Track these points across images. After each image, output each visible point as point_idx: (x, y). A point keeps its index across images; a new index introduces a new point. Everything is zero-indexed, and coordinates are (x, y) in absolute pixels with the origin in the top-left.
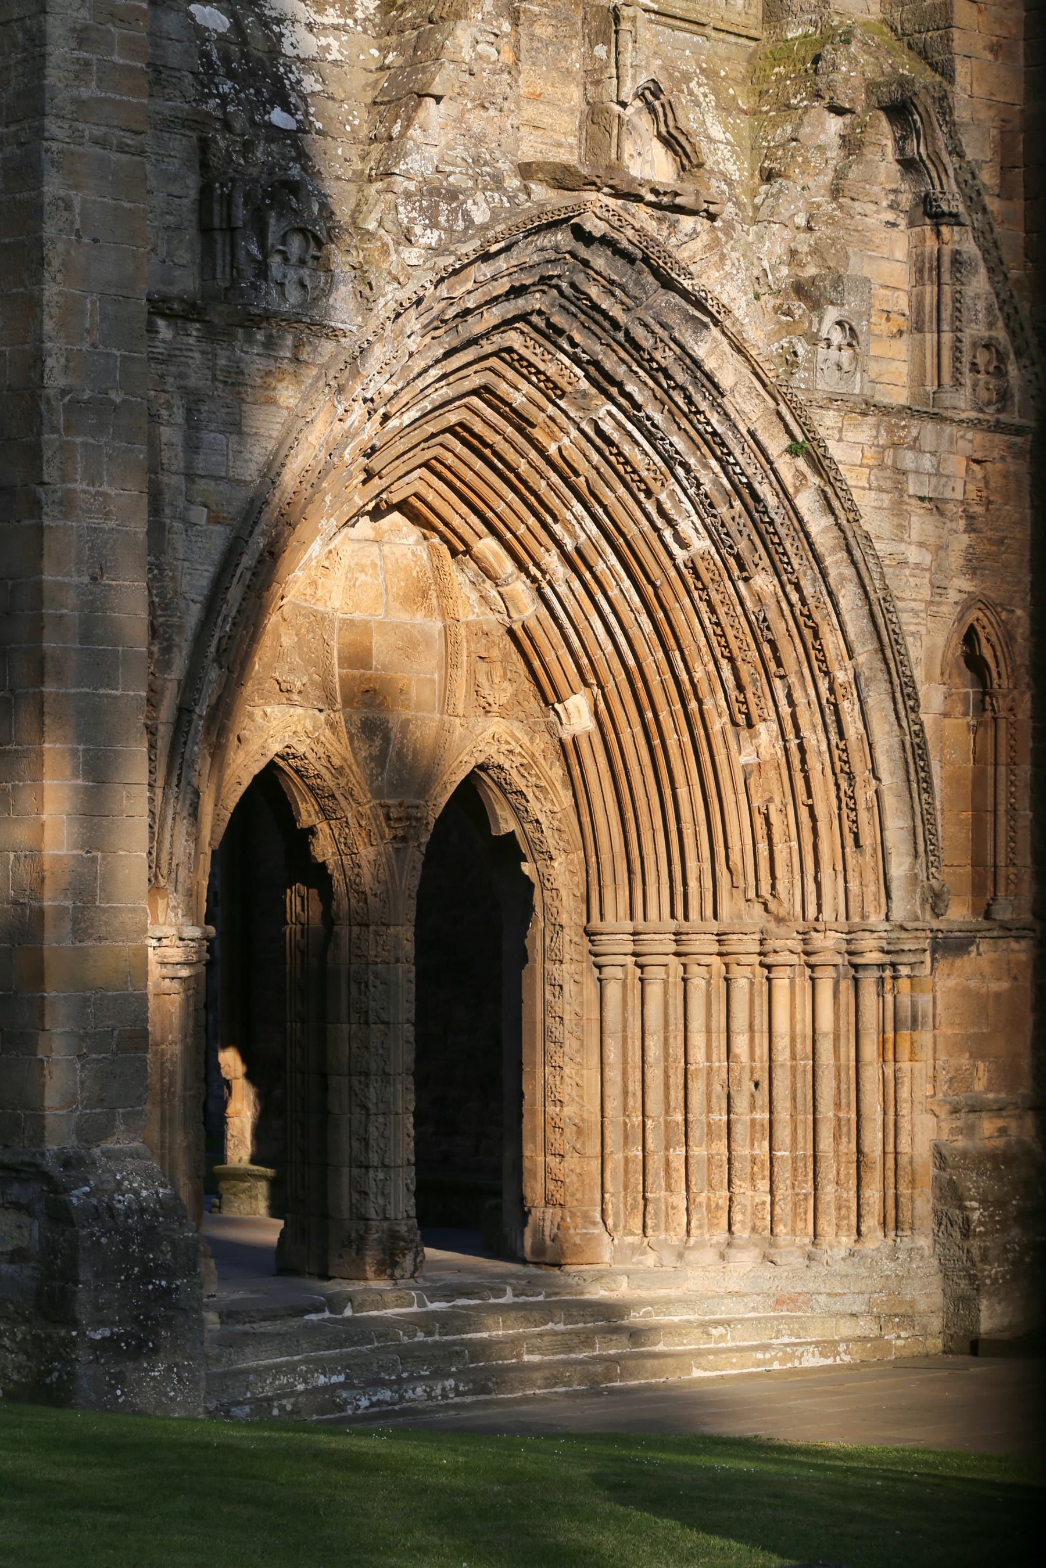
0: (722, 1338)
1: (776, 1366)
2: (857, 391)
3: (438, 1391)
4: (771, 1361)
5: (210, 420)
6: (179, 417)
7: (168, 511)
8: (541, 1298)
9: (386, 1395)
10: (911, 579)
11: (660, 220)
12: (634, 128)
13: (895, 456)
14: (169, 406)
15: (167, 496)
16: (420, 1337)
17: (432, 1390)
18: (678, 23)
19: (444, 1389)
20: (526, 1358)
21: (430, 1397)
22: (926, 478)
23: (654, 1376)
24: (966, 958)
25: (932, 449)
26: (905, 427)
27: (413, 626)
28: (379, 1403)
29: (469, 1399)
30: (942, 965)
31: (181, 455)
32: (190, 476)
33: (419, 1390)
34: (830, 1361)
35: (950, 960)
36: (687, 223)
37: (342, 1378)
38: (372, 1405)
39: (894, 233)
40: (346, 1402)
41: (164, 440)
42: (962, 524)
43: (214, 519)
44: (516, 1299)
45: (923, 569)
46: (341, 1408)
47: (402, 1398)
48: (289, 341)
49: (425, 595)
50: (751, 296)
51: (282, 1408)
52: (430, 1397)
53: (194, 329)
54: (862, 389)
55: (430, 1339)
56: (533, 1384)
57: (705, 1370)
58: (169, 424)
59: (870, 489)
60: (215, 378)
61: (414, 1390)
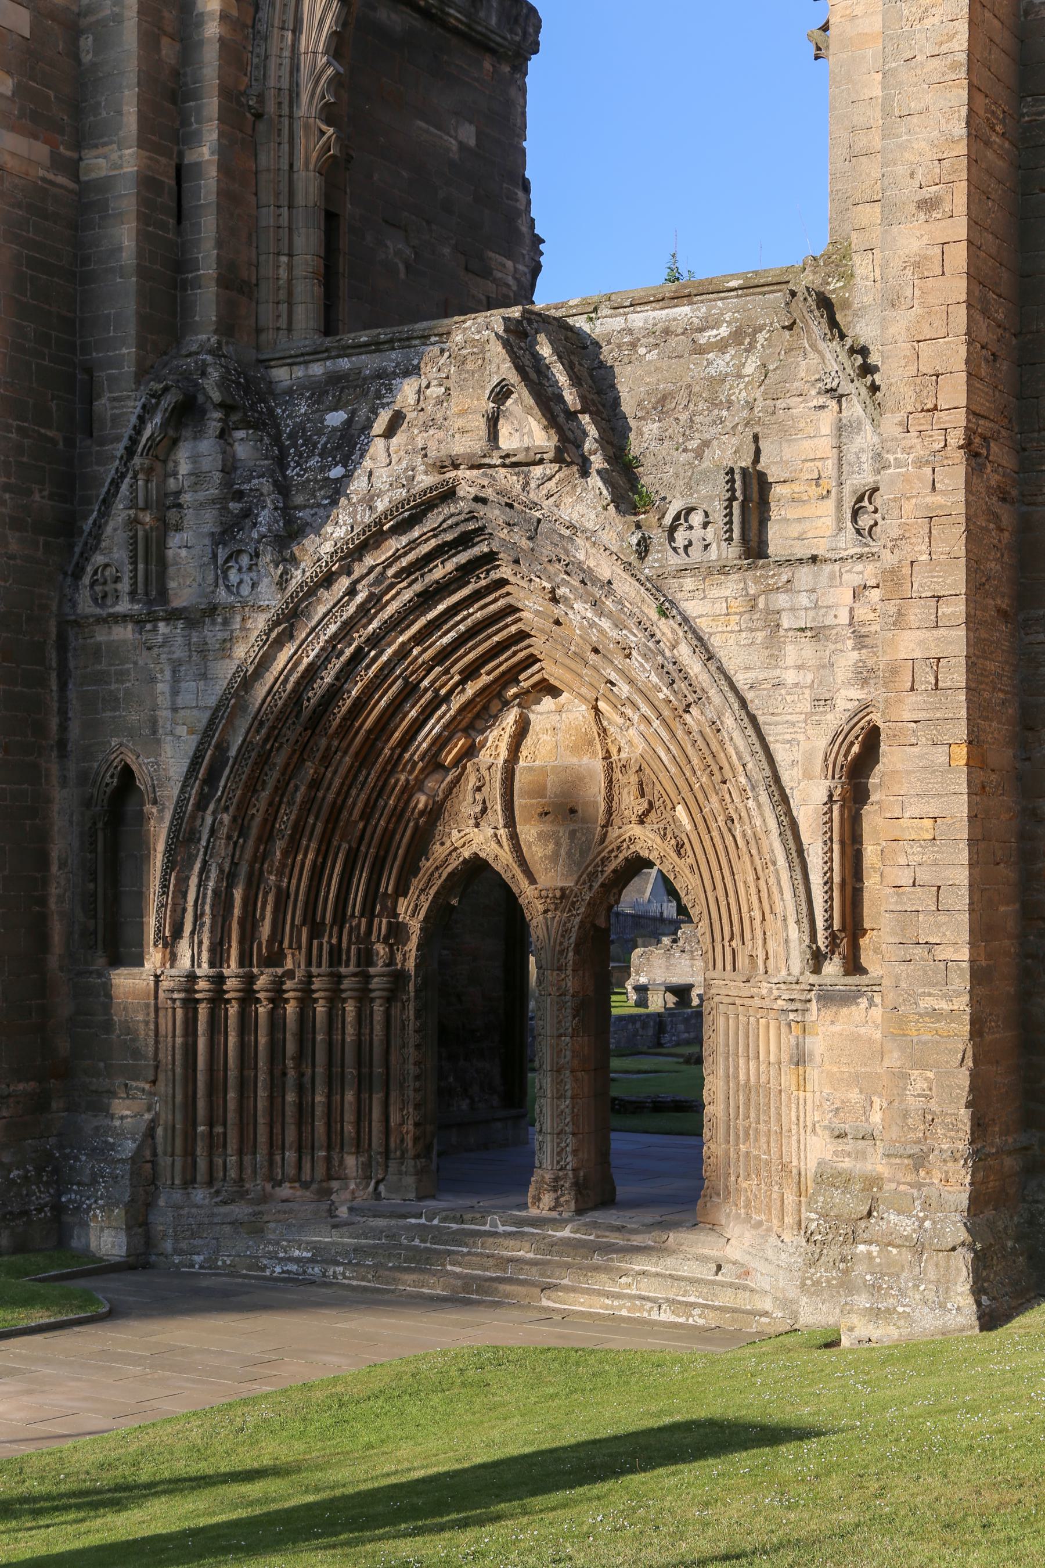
0: (629, 1285)
1: (624, 1313)
2: (714, 557)
3: (331, 1273)
4: (620, 1308)
5: (186, 675)
6: (168, 675)
7: (161, 731)
8: (592, 1238)
9: (294, 1267)
10: (788, 697)
11: (517, 474)
12: (511, 413)
13: (767, 600)
14: (162, 671)
15: (161, 723)
16: (417, 1242)
17: (326, 1271)
18: (766, 289)
19: (334, 1272)
20: (449, 1268)
21: (324, 1275)
22: (803, 613)
23: (507, 1297)
24: (854, 1008)
25: (809, 588)
26: (774, 575)
27: (580, 766)
28: (288, 1272)
29: (355, 1283)
30: (828, 1014)
31: (168, 698)
32: (175, 709)
33: (316, 1269)
34: (682, 1320)
35: (834, 1009)
36: (537, 471)
37: (309, 1255)
38: (283, 1272)
40: (266, 1266)
41: (158, 691)
42: (850, 643)
43: (191, 732)
44: (573, 1235)
45: (802, 687)
46: (263, 1269)
47: (305, 1272)
48: (238, 618)
49: (591, 743)
50: (600, 509)
51: (224, 1262)
52: (324, 1275)
53: (180, 624)
54: (719, 555)
55: (423, 1245)
56: (404, 1283)
57: (555, 1302)
58: (162, 681)
59: (740, 631)
60: (190, 650)
61: (313, 1269)
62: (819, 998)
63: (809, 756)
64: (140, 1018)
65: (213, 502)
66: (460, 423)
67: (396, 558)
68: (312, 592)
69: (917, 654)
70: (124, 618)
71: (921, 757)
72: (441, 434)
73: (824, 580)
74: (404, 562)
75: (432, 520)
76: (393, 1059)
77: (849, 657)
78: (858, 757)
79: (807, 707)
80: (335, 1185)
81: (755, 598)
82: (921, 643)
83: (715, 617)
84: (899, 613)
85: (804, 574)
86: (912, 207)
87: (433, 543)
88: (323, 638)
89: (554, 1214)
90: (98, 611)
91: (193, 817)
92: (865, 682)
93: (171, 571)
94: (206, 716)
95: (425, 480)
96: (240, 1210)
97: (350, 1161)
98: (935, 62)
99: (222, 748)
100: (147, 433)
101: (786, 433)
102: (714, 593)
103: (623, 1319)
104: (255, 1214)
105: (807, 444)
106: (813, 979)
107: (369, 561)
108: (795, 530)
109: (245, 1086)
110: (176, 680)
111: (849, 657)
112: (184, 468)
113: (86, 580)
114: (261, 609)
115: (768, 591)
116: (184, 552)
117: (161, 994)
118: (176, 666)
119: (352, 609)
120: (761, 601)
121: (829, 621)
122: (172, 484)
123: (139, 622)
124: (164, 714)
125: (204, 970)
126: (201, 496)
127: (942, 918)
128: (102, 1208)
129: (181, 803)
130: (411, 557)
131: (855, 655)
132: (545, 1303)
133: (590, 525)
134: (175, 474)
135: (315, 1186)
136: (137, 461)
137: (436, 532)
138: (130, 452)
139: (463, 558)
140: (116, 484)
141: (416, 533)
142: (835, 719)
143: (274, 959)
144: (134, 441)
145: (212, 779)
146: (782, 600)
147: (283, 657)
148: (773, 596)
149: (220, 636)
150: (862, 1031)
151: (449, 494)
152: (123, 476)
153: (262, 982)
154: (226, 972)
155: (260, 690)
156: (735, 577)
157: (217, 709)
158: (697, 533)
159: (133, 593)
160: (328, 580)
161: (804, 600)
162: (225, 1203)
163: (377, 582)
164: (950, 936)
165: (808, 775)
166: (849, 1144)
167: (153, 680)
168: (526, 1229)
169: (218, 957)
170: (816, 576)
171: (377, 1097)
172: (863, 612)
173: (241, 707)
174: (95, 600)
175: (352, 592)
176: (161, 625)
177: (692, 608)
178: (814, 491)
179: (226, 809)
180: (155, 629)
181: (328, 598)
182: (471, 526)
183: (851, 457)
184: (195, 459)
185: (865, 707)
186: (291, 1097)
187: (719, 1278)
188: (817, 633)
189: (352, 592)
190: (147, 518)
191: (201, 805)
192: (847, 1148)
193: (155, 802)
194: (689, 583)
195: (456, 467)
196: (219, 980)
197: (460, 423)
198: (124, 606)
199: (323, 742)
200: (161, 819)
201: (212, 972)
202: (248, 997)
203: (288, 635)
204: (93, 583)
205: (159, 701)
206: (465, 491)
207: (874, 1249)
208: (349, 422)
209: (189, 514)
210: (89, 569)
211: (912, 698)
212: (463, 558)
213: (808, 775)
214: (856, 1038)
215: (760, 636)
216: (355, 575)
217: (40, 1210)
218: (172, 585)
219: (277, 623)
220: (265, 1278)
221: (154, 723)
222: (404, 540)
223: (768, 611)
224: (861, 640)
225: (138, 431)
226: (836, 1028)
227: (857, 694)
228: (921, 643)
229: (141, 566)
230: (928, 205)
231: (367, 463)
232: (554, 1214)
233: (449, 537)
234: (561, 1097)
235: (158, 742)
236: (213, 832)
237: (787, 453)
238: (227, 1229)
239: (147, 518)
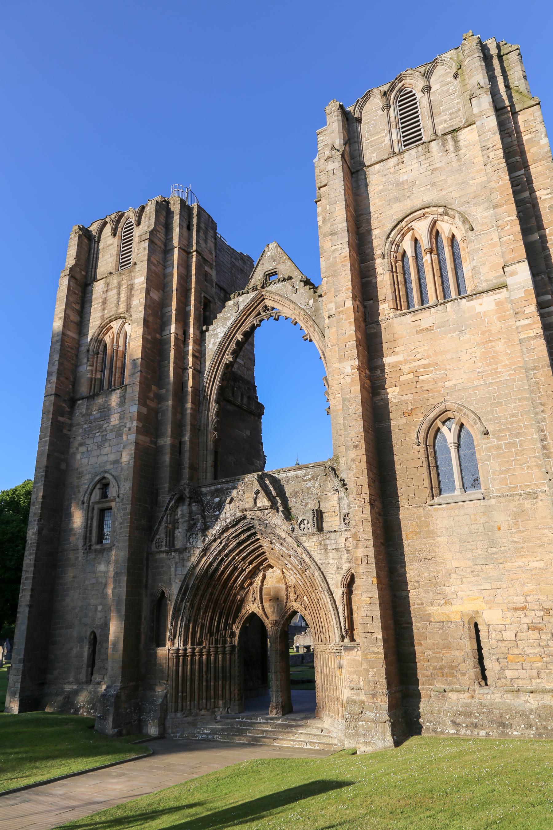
0: (298, 737)
1: (297, 746)
4: (295, 744)
6: (174, 566)
9: (205, 736)
16: (239, 726)
30: (347, 653)
32: (176, 575)
34: (313, 748)
36: (266, 511)
39: (335, 495)
42: (345, 552)
43: (180, 581)
46: (196, 737)
49: (282, 580)
53: (178, 553)
62: (344, 649)
63: (337, 583)
64: (164, 662)
65: (187, 521)
66: (247, 500)
67: (232, 534)
68: (211, 543)
69: (362, 555)
70: (163, 552)
71: (365, 581)
72: (242, 503)
73: (338, 537)
74: (234, 535)
75: (241, 524)
76: (232, 671)
77: (346, 556)
78: (349, 582)
79: (335, 569)
80: (216, 710)
81: (321, 541)
82: (363, 552)
83: (311, 546)
84: (357, 544)
85: (333, 535)
86: (352, 447)
87: (241, 530)
88: (214, 555)
89: (276, 716)
90: (157, 550)
91: (180, 604)
92: (350, 562)
93: (176, 539)
94: (184, 576)
95: (239, 514)
96: (190, 719)
97: (221, 702)
98: (355, 415)
99: (187, 585)
100: (171, 505)
101: (326, 500)
102: (311, 540)
103: (296, 748)
104: (194, 720)
105: (331, 503)
106: (342, 643)
107: (225, 535)
108: (330, 524)
109: (192, 681)
110: (176, 567)
111: (346, 556)
112: (180, 513)
113: (154, 542)
114: (198, 548)
115: (324, 540)
116: (179, 534)
117: (170, 655)
118: (176, 563)
119: (221, 547)
120: (323, 542)
121: (340, 547)
122: (176, 517)
123: (167, 552)
124: (173, 576)
125: (182, 647)
126: (184, 520)
127: (374, 625)
128: (152, 720)
129: (177, 600)
130: (236, 534)
131: (347, 555)
132: (275, 744)
133: (279, 524)
134: (177, 515)
135: (211, 710)
136: (168, 512)
137: (242, 527)
138: (166, 509)
139: (248, 533)
140: (162, 518)
141: (237, 528)
142: (343, 572)
143: (200, 643)
144: (167, 507)
145: (184, 594)
146: (328, 542)
147: (203, 560)
148: (325, 541)
149: (188, 555)
150: (356, 658)
151: (245, 518)
152: (164, 515)
153: (197, 650)
154: (187, 647)
155: (198, 569)
156: (316, 536)
157: (187, 574)
158: (306, 525)
159: (166, 546)
160: (215, 540)
161: (333, 541)
162: (186, 717)
163: (227, 540)
164: (377, 630)
165: (337, 587)
166: (355, 692)
167: (170, 568)
168: (269, 721)
169: (185, 644)
170: (336, 535)
171: (228, 683)
172: (348, 544)
173: (193, 574)
174: (156, 547)
175: (221, 543)
176: (173, 553)
177: (305, 544)
178: (334, 514)
179: (188, 602)
180: (171, 554)
181: (215, 545)
182: (250, 525)
183: (342, 506)
184: (182, 511)
185: (350, 569)
186: (204, 684)
187: (322, 734)
188: (337, 550)
189: (221, 543)
190: (170, 526)
191: (182, 601)
192: (355, 692)
193: (170, 600)
194: (305, 538)
195: (246, 511)
196: (185, 650)
197: (247, 500)
198: (164, 549)
199: (213, 583)
200: (171, 605)
201: (184, 648)
202: (193, 655)
203: (205, 555)
204: (156, 543)
205: (172, 573)
206: (249, 517)
207: (364, 723)
208: (220, 501)
209: (180, 524)
210: (155, 539)
211: (362, 566)
212: (248, 533)
213: (337, 587)
214: (354, 660)
215: (323, 551)
216: (222, 539)
217: (134, 721)
218: (176, 543)
219: (202, 552)
220: (197, 740)
221: (170, 579)
222: (234, 529)
223: (324, 545)
224: (348, 551)
225: (169, 504)
226: (349, 657)
227: (348, 565)
228: (363, 552)
229: (168, 538)
230: (356, 447)
231: (225, 511)
232: (276, 716)
233: (245, 528)
234: (277, 680)
235: (171, 584)
236: (185, 608)
237: (327, 505)
238: (186, 725)
239: (170, 526)
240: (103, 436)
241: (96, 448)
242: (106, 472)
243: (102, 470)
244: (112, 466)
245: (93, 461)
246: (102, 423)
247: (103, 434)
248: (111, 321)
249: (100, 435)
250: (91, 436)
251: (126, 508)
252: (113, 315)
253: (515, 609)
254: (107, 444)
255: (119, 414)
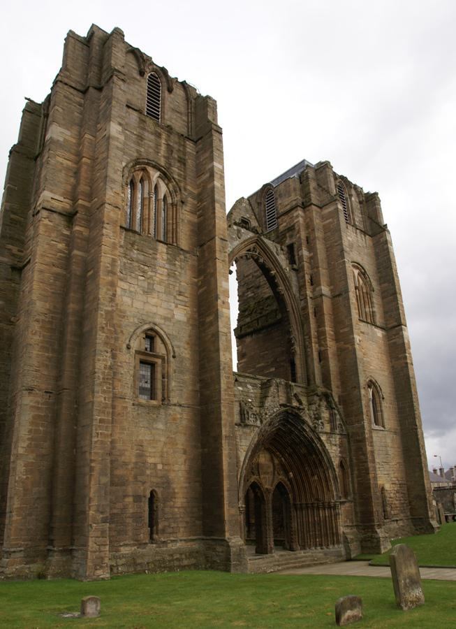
118: (241, 436)
240: (149, 284)
241: (141, 292)
242: (156, 325)
243: (150, 320)
244: (162, 321)
245: (138, 305)
246: (146, 268)
247: (149, 281)
248: (148, 164)
249: (144, 280)
250: (133, 275)
251: (229, 377)
252: (153, 161)
253: (393, 484)
254: (155, 295)
255: (166, 270)
